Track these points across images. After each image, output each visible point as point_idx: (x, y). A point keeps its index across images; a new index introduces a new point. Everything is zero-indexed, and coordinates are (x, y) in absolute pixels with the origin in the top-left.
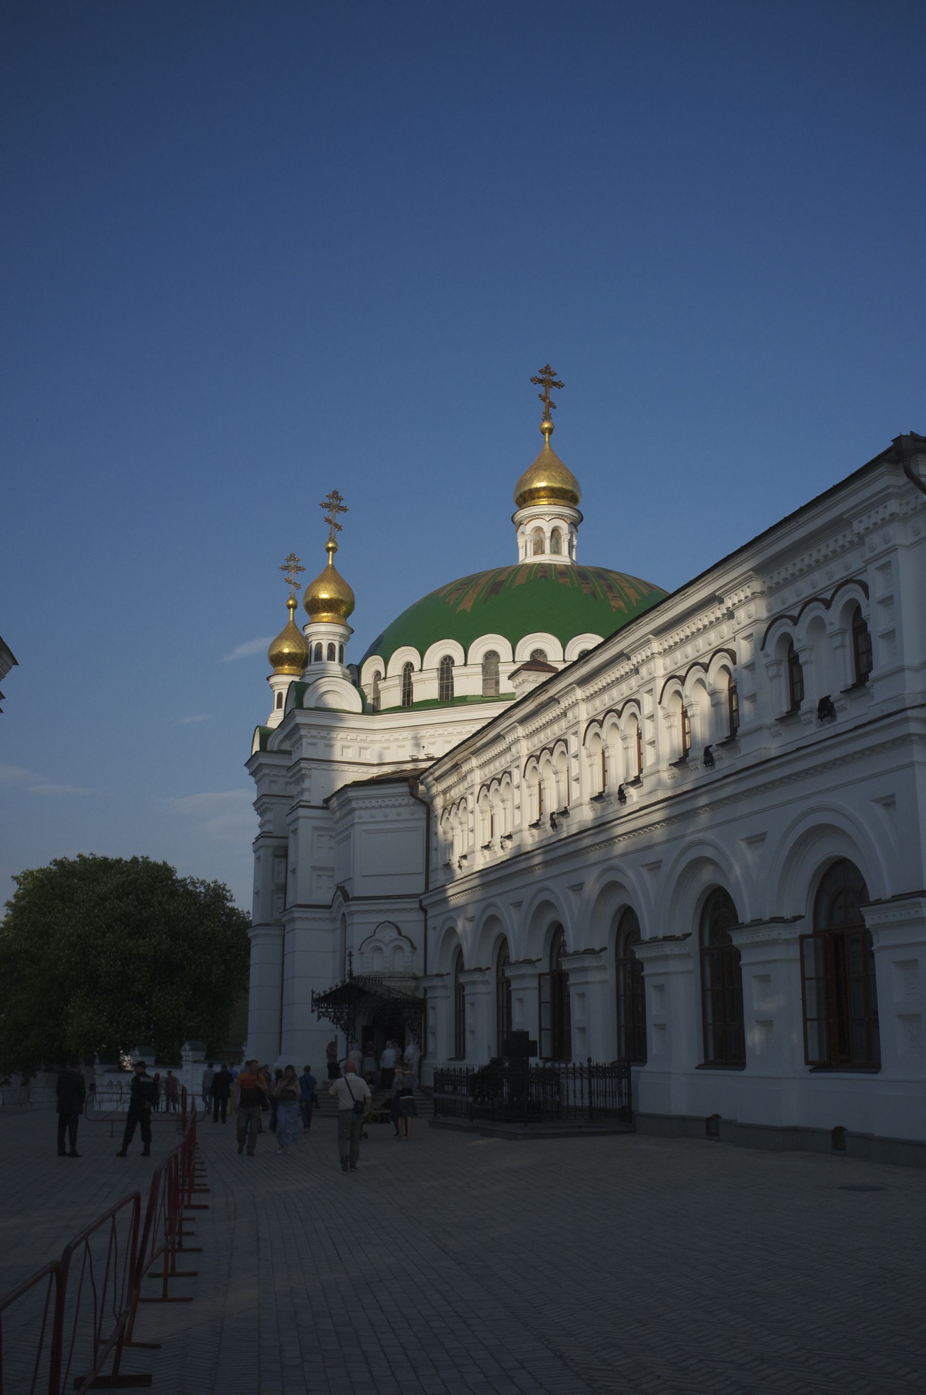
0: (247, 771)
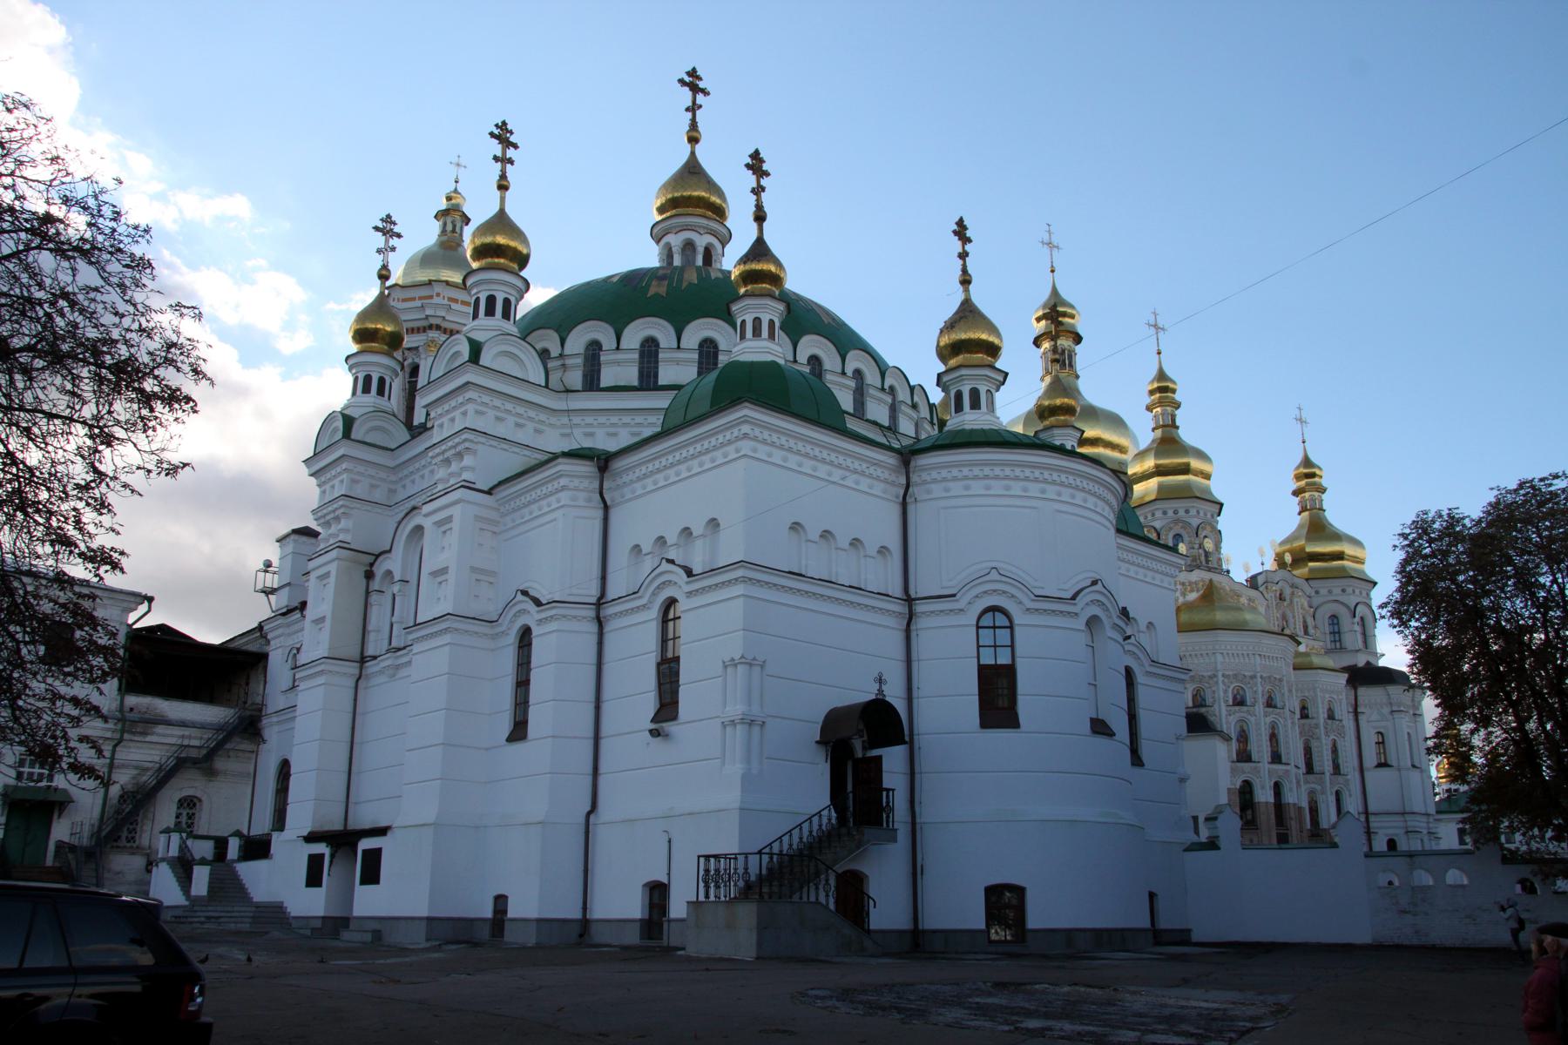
0: (305, 470)
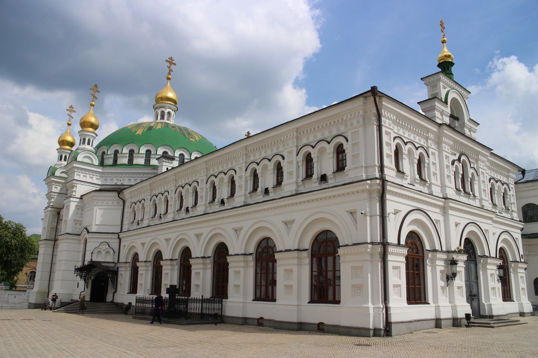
0: (44, 182)
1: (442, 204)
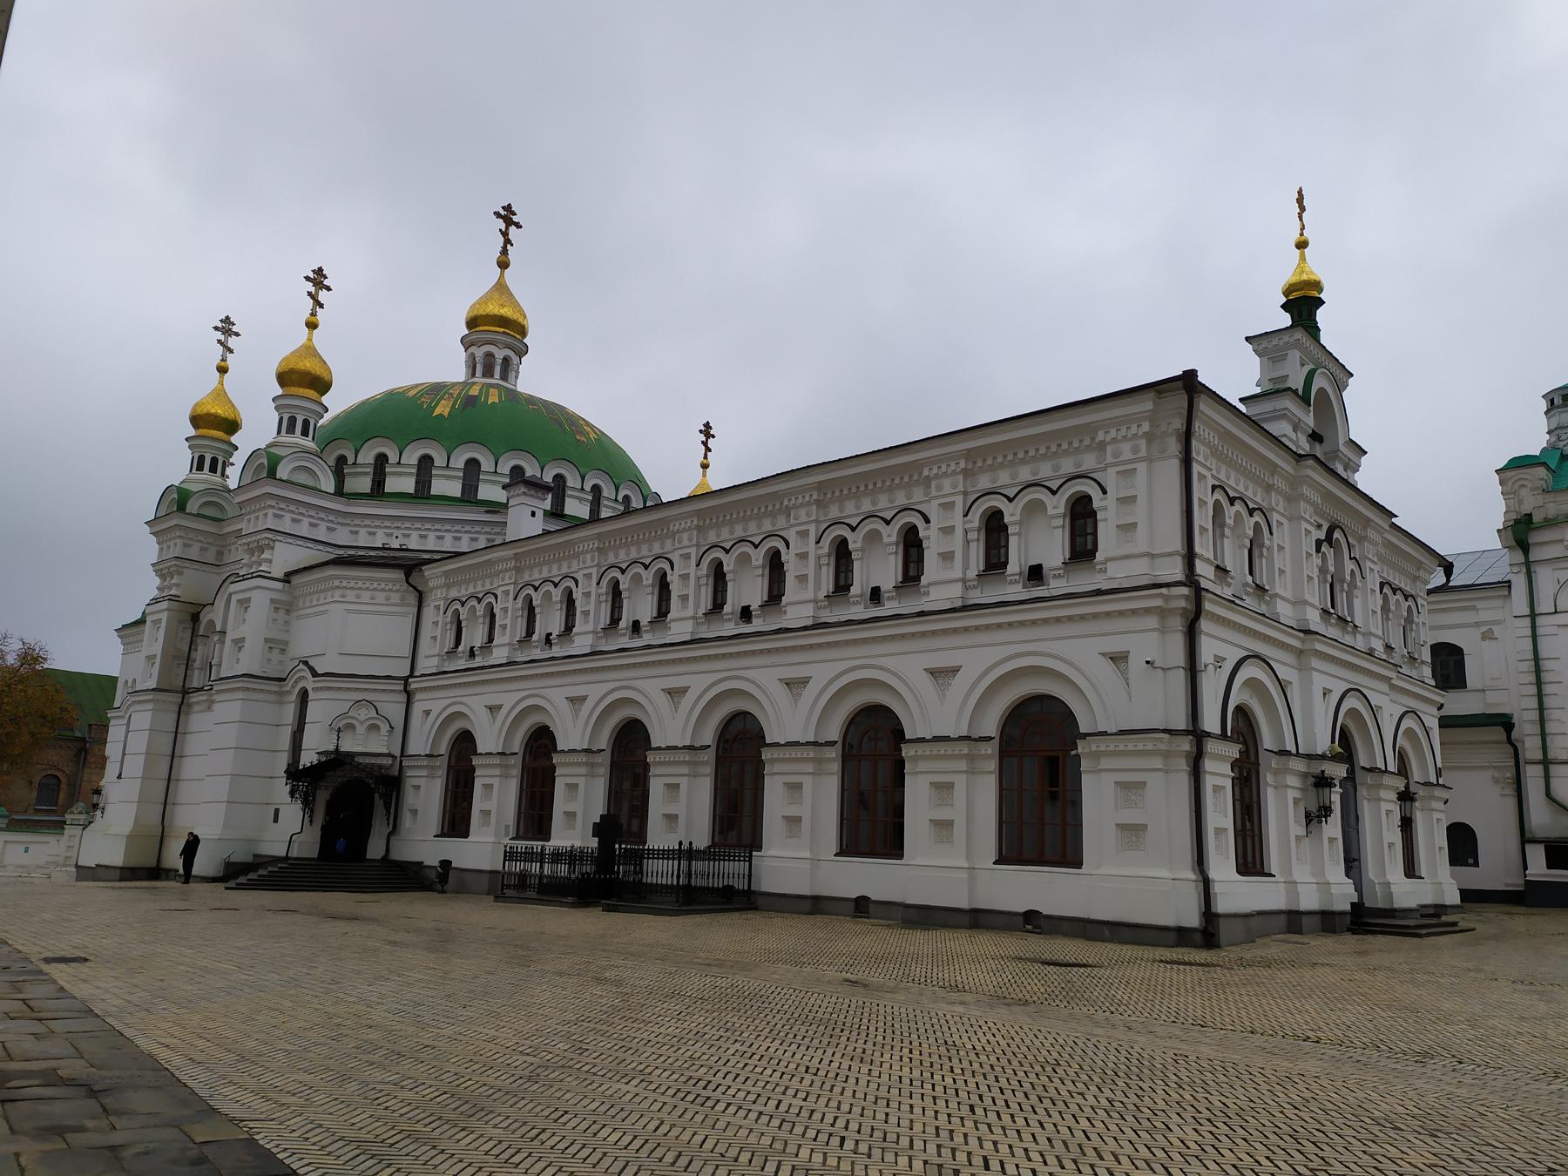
1: (1296, 643)
